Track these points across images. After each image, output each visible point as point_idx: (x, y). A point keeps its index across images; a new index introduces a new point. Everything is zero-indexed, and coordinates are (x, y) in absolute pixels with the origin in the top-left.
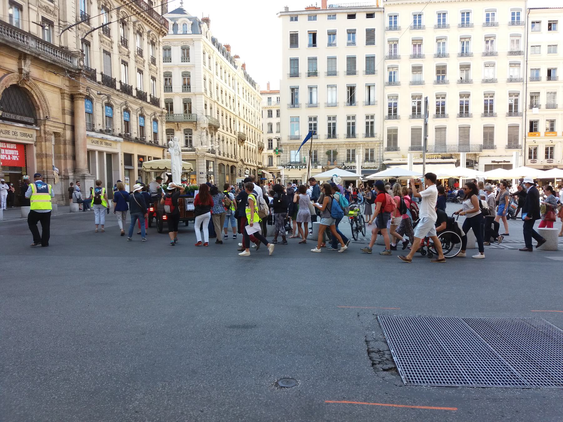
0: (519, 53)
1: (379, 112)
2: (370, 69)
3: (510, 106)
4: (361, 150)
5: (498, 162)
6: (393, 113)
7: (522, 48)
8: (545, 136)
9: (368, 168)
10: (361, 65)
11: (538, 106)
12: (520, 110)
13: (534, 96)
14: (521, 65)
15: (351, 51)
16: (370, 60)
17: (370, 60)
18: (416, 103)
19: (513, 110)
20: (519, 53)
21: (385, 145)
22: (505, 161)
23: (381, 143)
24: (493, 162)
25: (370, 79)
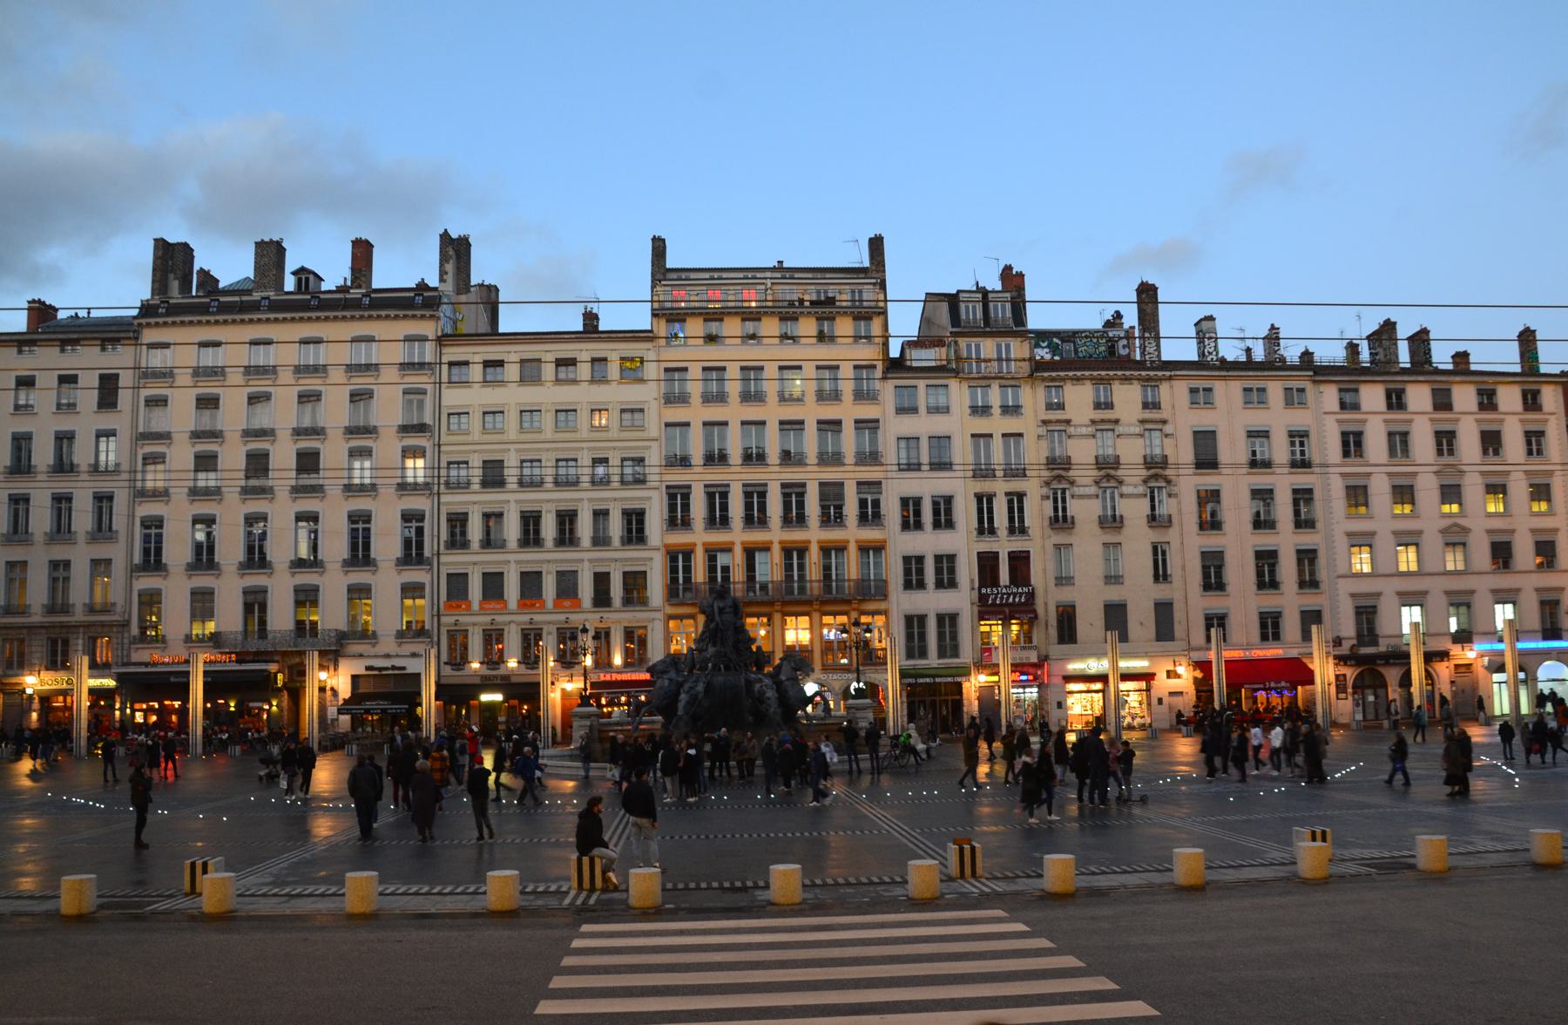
0: (421, 428)
3: (407, 543)
5: (380, 669)
7: (428, 419)
8: (481, 608)
11: (502, 545)
12: (427, 553)
13: (458, 522)
14: (428, 454)
19: (413, 553)
20: (421, 428)
22: (394, 668)
24: (368, 668)
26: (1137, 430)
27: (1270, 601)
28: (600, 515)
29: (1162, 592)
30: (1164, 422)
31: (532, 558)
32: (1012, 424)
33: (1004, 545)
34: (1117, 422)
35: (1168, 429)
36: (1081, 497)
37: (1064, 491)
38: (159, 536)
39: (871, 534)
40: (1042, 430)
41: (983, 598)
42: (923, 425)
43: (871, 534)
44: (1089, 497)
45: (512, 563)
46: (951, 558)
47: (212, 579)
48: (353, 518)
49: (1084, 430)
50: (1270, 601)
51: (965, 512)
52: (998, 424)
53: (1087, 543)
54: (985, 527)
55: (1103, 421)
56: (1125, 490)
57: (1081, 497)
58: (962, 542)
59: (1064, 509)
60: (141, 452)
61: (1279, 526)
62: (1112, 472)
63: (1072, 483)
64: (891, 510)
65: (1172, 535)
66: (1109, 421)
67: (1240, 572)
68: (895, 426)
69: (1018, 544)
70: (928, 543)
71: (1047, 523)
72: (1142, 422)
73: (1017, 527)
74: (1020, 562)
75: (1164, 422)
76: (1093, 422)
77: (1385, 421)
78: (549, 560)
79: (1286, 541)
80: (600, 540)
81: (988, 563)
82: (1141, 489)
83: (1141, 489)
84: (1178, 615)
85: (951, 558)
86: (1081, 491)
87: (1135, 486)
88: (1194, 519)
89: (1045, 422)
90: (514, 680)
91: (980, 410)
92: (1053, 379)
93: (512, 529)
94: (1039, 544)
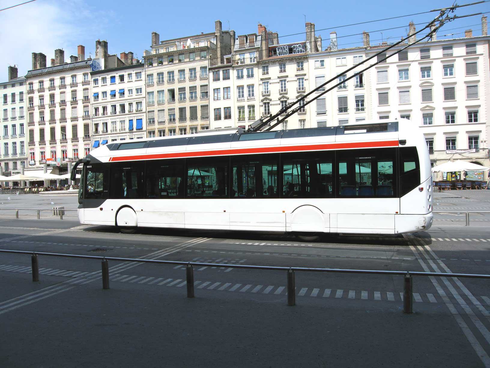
30: (305, 75)
32: (250, 81)
35: (305, 77)
37: (268, 103)
40: (261, 82)
51: (235, 113)
52: (245, 82)
59: (269, 110)
61: (349, 111)
63: (271, 100)
68: (213, 85)
75: (305, 75)
76: (279, 78)
77: (397, 66)
91: (240, 77)
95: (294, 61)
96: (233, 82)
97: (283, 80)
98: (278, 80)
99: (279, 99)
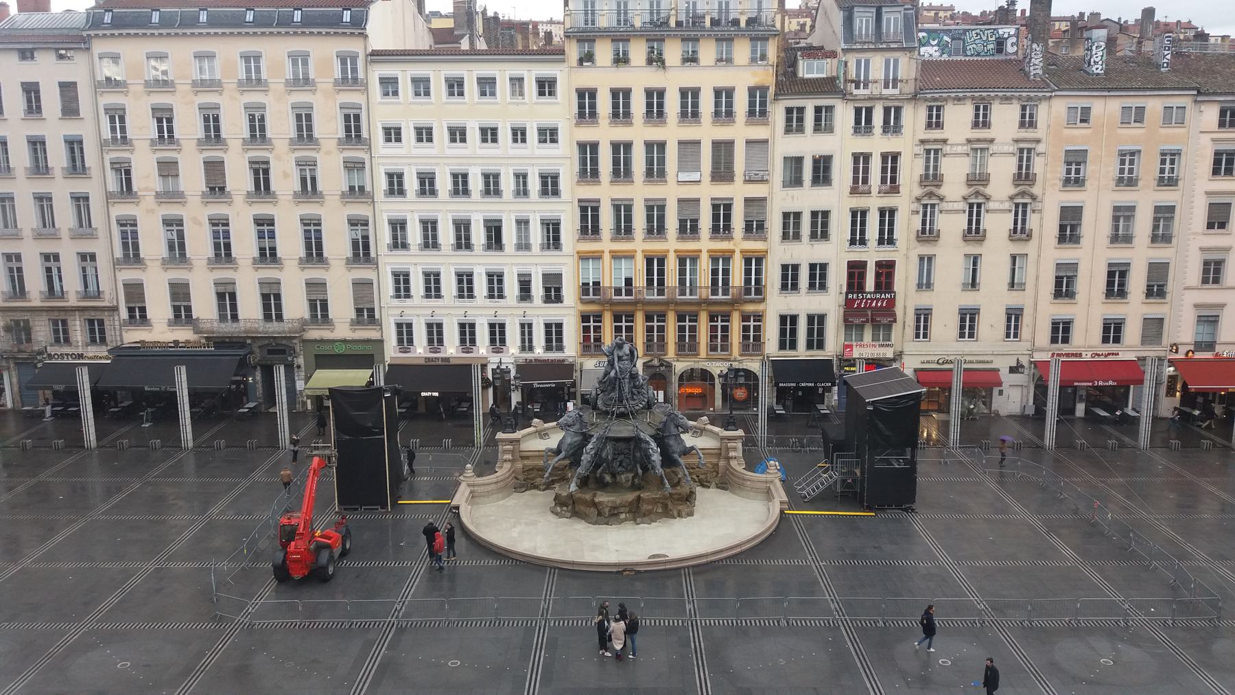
1: (106, 247)
2: (77, 167)
3: (355, 244)
4: (78, 323)
6: (131, 253)
9: (95, 357)
10: (57, 157)
15: (35, 129)
16: (74, 146)
17: (74, 146)
18: (175, 233)
19: (362, 251)
21: (124, 314)
23: (115, 309)
25: (80, 186)
26: (1011, 149)
27: (1115, 310)
28: (522, 223)
29: (1014, 299)
30: (1038, 141)
31: (464, 261)
33: (871, 255)
34: (992, 141)
35: (1041, 148)
36: (948, 212)
38: (135, 233)
39: (755, 245)
41: (849, 303)
42: (808, 145)
43: (755, 245)
44: (957, 211)
45: (448, 263)
46: (824, 267)
47: (185, 272)
48: (305, 222)
49: (959, 149)
50: (1115, 310)
51: (840, 226)
52: (877, 144)
53: (950, 257)
54: (858, 238)
55: (979, 140)
56: (991, 205)
57: (948, 212)
58: (835, 253)
60: (108, 158)
61: (1135, 241)
62: (981, 188)
64: (775, 225)
65: (1030, 248)
66: (985, 140)
67: (1091, 282)
69: (885, 254)
70: (804, 252)
71: (913, 236)
72: (1017, 141)
73: (886, 238)
74: (886, 270)
75: (1038, 141)
76: (969, 141)
78: (480, 263)
79: (1140, 256)
80: (524, 246)
81: (856, 271)
82: (1007, 205)
83: (1007, 205)
84: (1026, 319)
85: (824, 267)
86: (950, 206)
87: (1002, 202)
88: (1055, 231)
89: (923, 142)
90: (453, 362)
92: (935, 100)
93: (446, 235)
94: (905, 256)
95: (1015, 101)
96: (841, 143)
97: (979, 148)
98: (966, 149)
99: (965, 199)
